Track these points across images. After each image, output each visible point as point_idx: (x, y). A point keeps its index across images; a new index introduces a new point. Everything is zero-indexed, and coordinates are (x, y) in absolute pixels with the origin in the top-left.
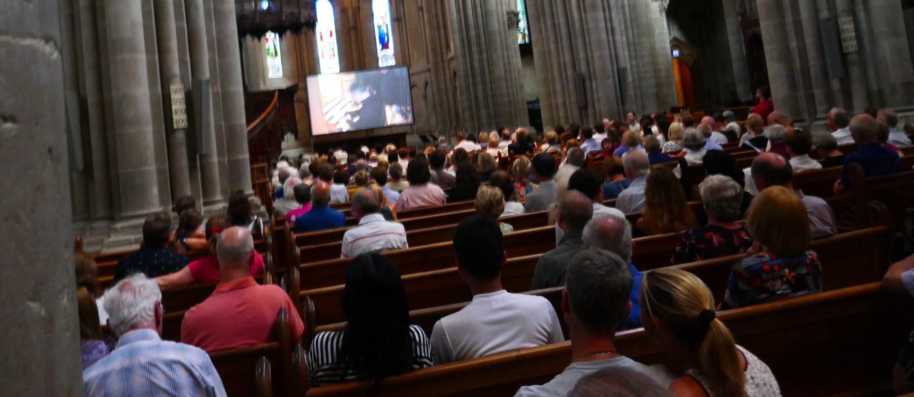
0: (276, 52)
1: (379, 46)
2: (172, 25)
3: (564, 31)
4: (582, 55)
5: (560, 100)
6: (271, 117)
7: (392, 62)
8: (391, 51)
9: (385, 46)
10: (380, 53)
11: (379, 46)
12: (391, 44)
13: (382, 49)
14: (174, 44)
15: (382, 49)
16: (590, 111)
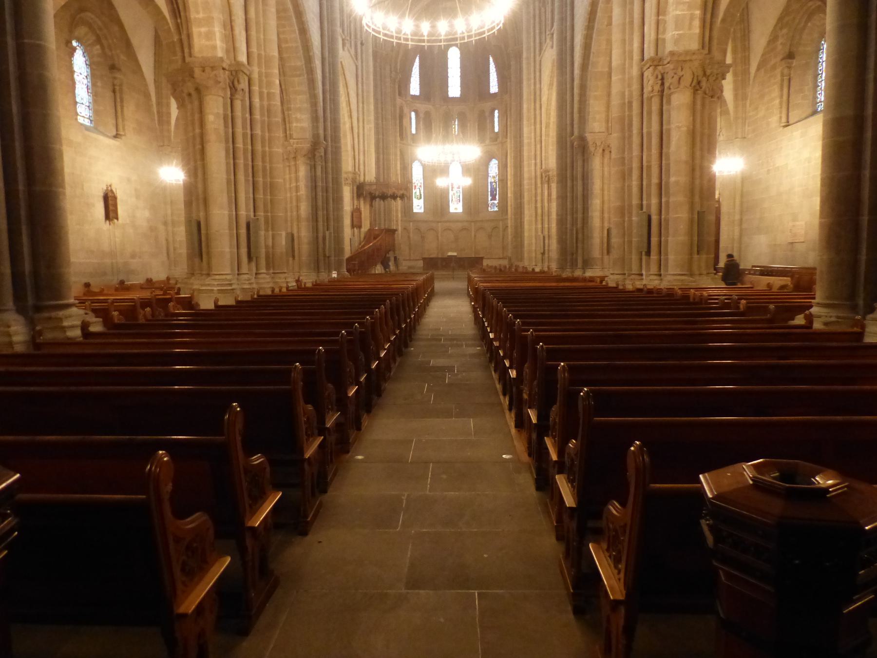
0: (421, 195)
1: (490, 198)
2: (320, 213)
3: (539, 211)
4: (546, 226)
5: (534, 248)
6: (379, 243)
7: (496, 209)
8: (496, 202)
9: (494, 198)
10: (490, 202)
11: (490, 198)
12: (497, 197)
13: (491, 200)
14: (320, 219)
15: (491, 200)
16: (546, 255)
